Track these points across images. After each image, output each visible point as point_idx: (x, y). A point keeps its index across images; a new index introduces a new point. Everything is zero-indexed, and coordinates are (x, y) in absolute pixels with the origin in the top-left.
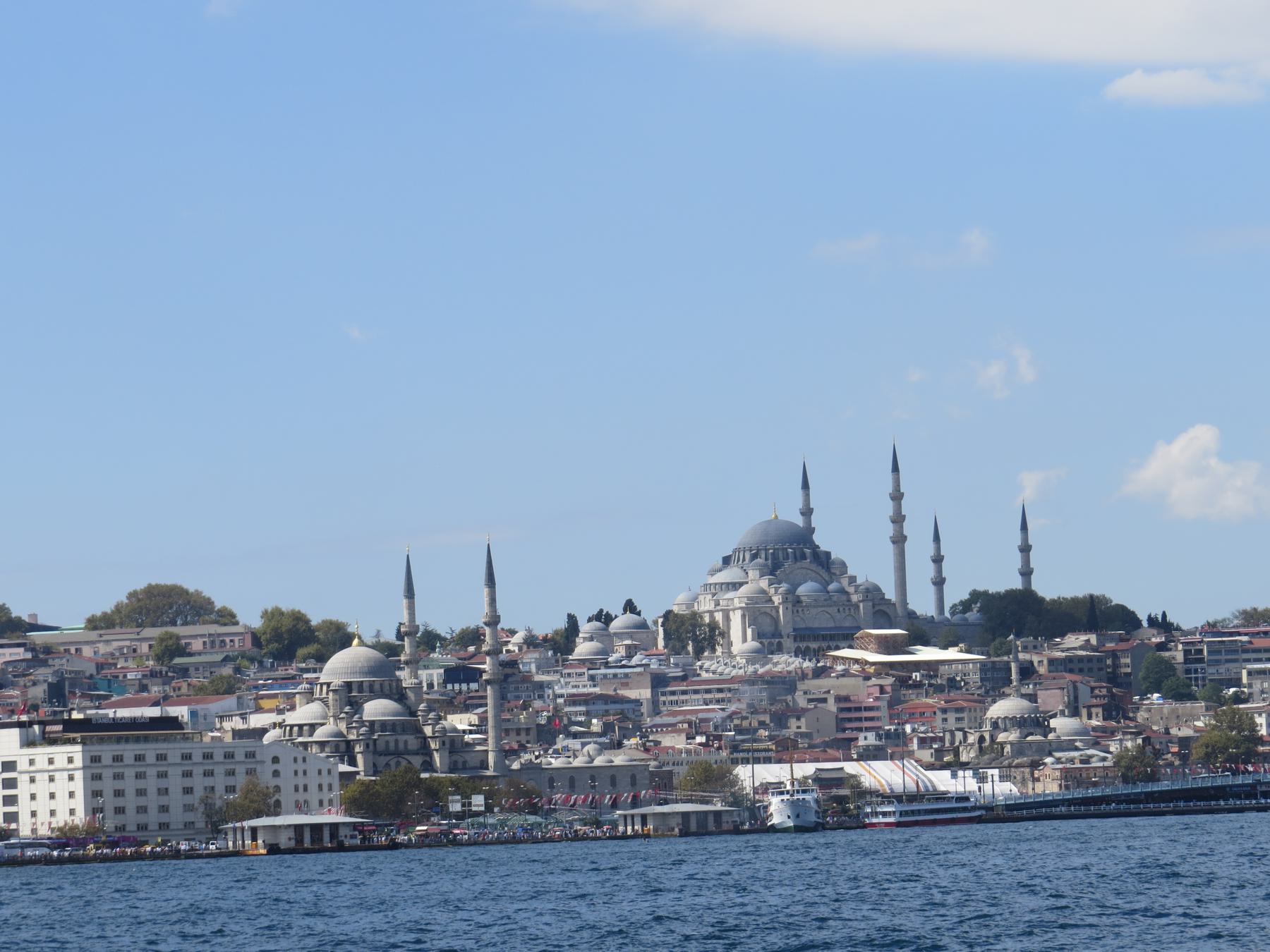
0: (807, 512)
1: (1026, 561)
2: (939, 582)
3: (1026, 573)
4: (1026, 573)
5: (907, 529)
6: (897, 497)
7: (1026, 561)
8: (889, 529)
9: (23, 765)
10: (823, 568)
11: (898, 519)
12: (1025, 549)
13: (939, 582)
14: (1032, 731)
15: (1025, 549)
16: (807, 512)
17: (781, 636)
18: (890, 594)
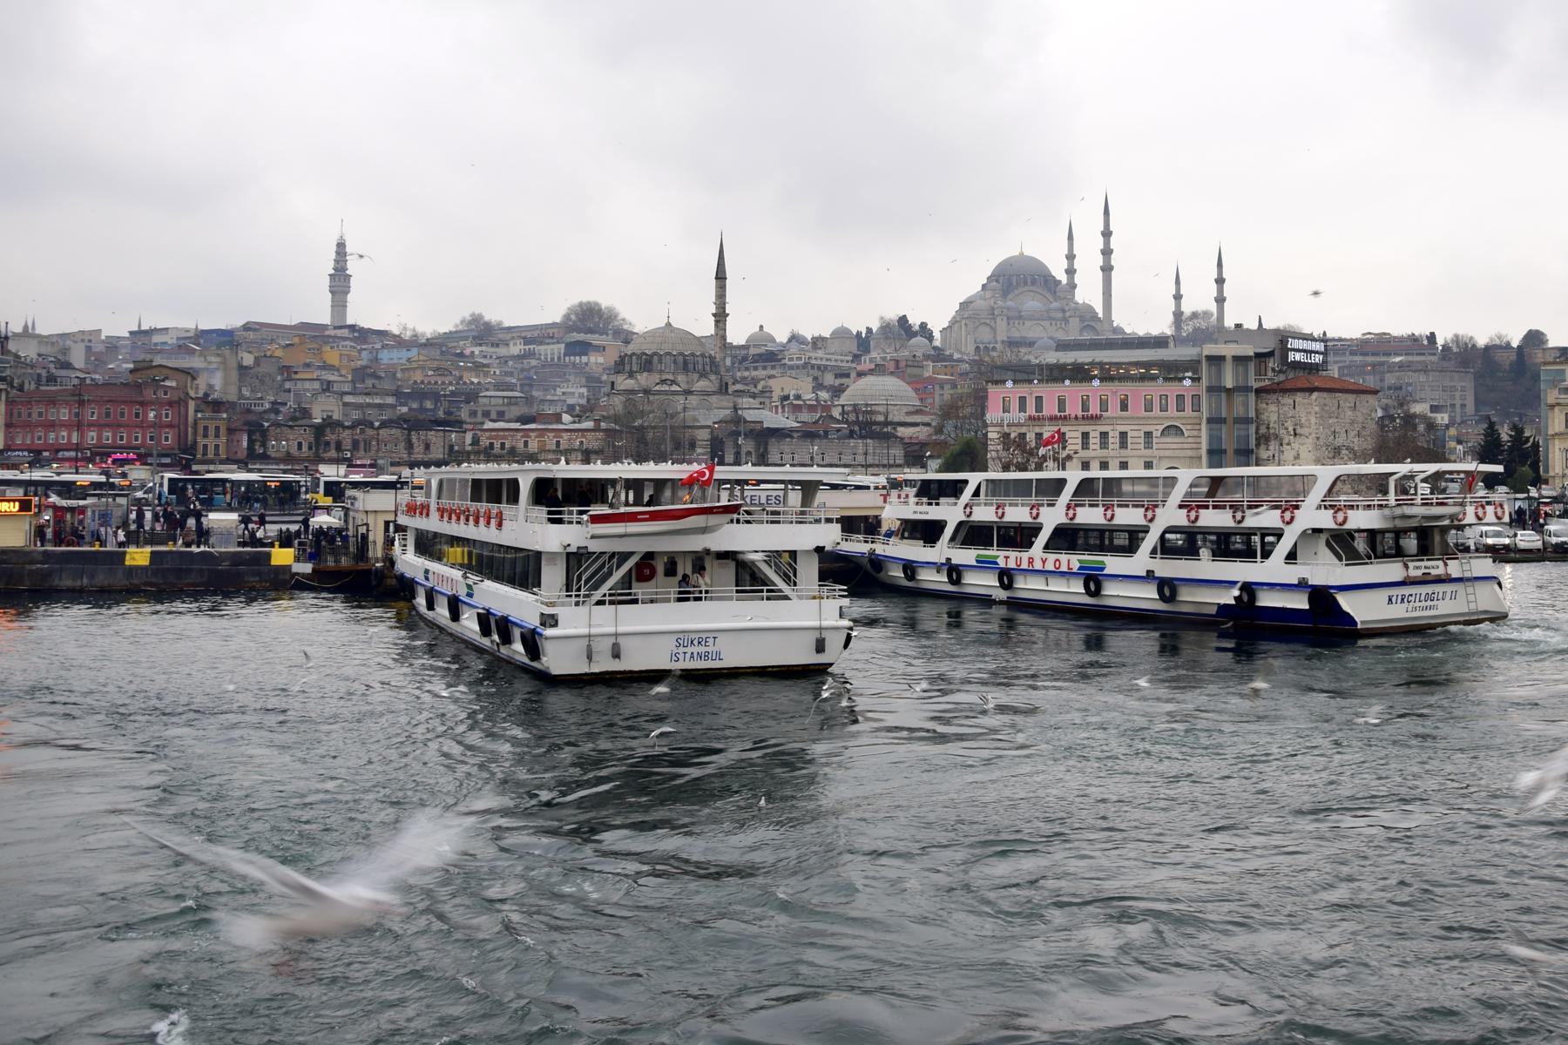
0: (1071, 257)
1: (1220, 290)
3: (1220, 300)
4: (1220, 300)
5: (1115, 260)
6: (1107, 234)
7: (1220, 290)
8: (1100, 260)
10: (1049, 290)
11: (1107, 252)
12: (1220, 281)
13: (1178, 314)
14: (670, 377)
15: (1220, 281)
16: (1071, 257)
17: (996, 342)
18: (1099, 311)
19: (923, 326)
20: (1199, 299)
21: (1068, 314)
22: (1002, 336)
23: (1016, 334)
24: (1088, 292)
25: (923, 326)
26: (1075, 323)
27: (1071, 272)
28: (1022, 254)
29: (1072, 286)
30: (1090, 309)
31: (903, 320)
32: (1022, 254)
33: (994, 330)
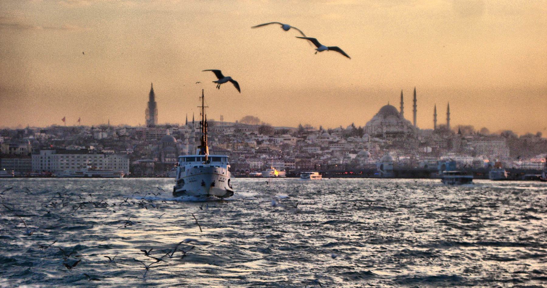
2: (435, 120)
3: (448, 119)
4: (448, 119)
9: (51, 158)
13: (435, 120)
19: (360, 127)
20: (441, 120)
21: (403, 124)
22: (385, 131)
23: (388, 130)
24: (408, 115)
25: (360, 127)
26: (405, 127)
27: (402, 108)
28: (389, 104)
29: (402, 112)
30: (409, 122)
31: (353, 125)
32: (389, 104)
33: (382, 129)
